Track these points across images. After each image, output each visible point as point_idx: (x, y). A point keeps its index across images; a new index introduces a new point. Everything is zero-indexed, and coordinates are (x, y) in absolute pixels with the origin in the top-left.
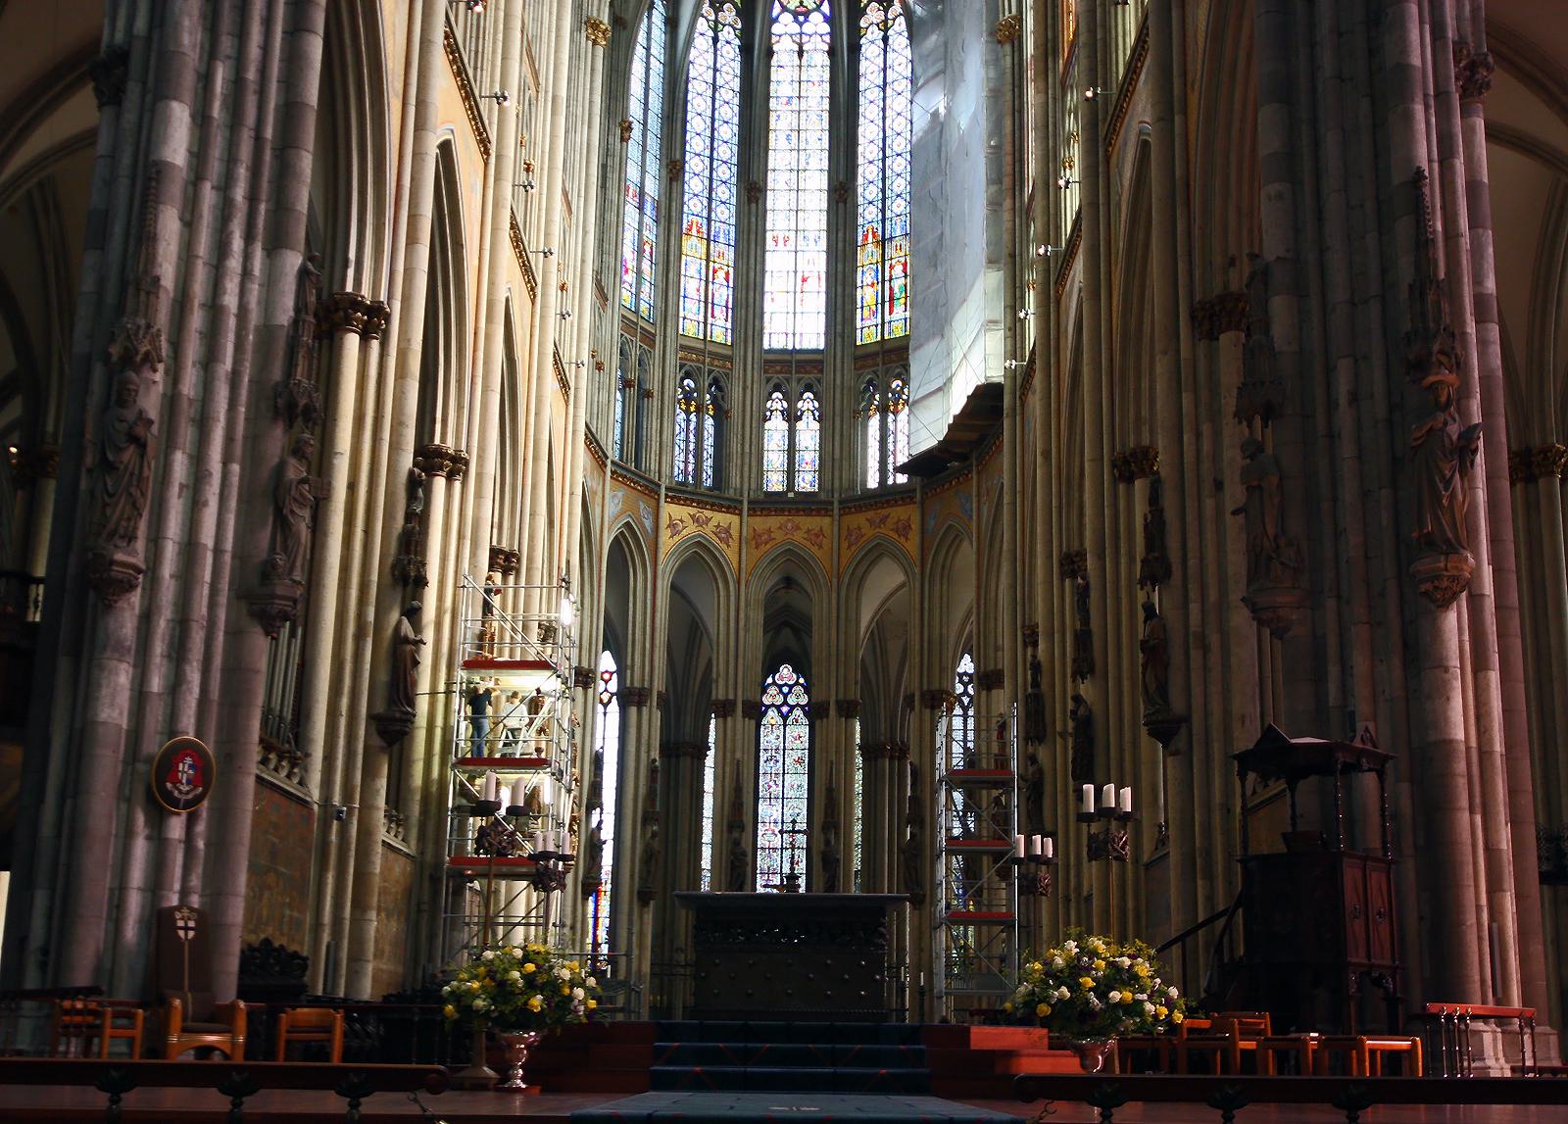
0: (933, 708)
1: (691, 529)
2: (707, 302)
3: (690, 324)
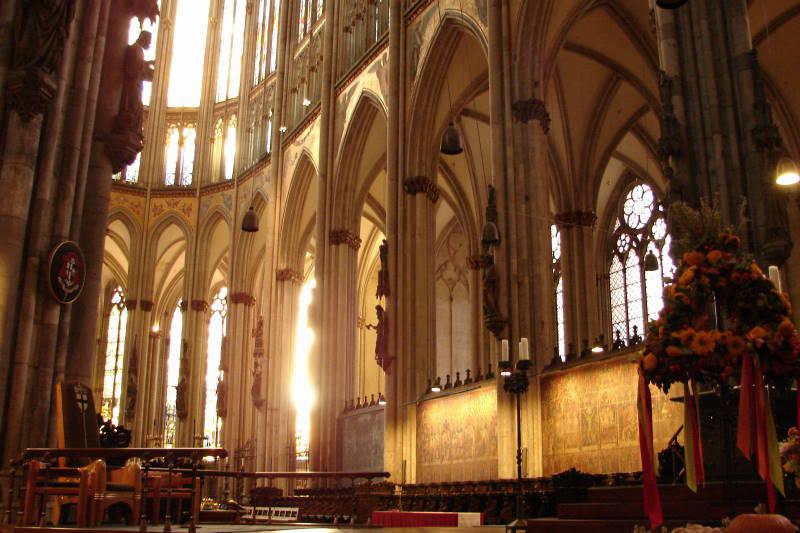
0: (198, 310)
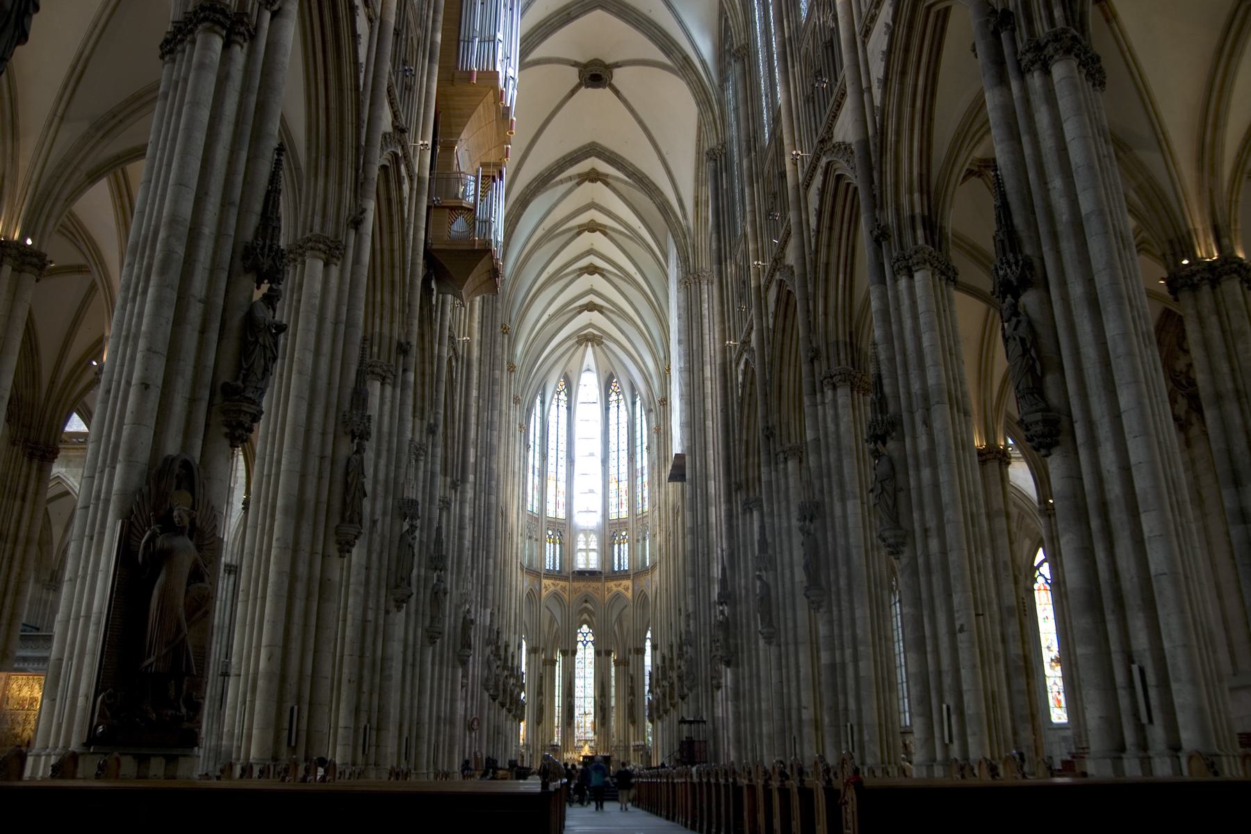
1: (552, 588)
2: (557, 504)
3: (551, 513)
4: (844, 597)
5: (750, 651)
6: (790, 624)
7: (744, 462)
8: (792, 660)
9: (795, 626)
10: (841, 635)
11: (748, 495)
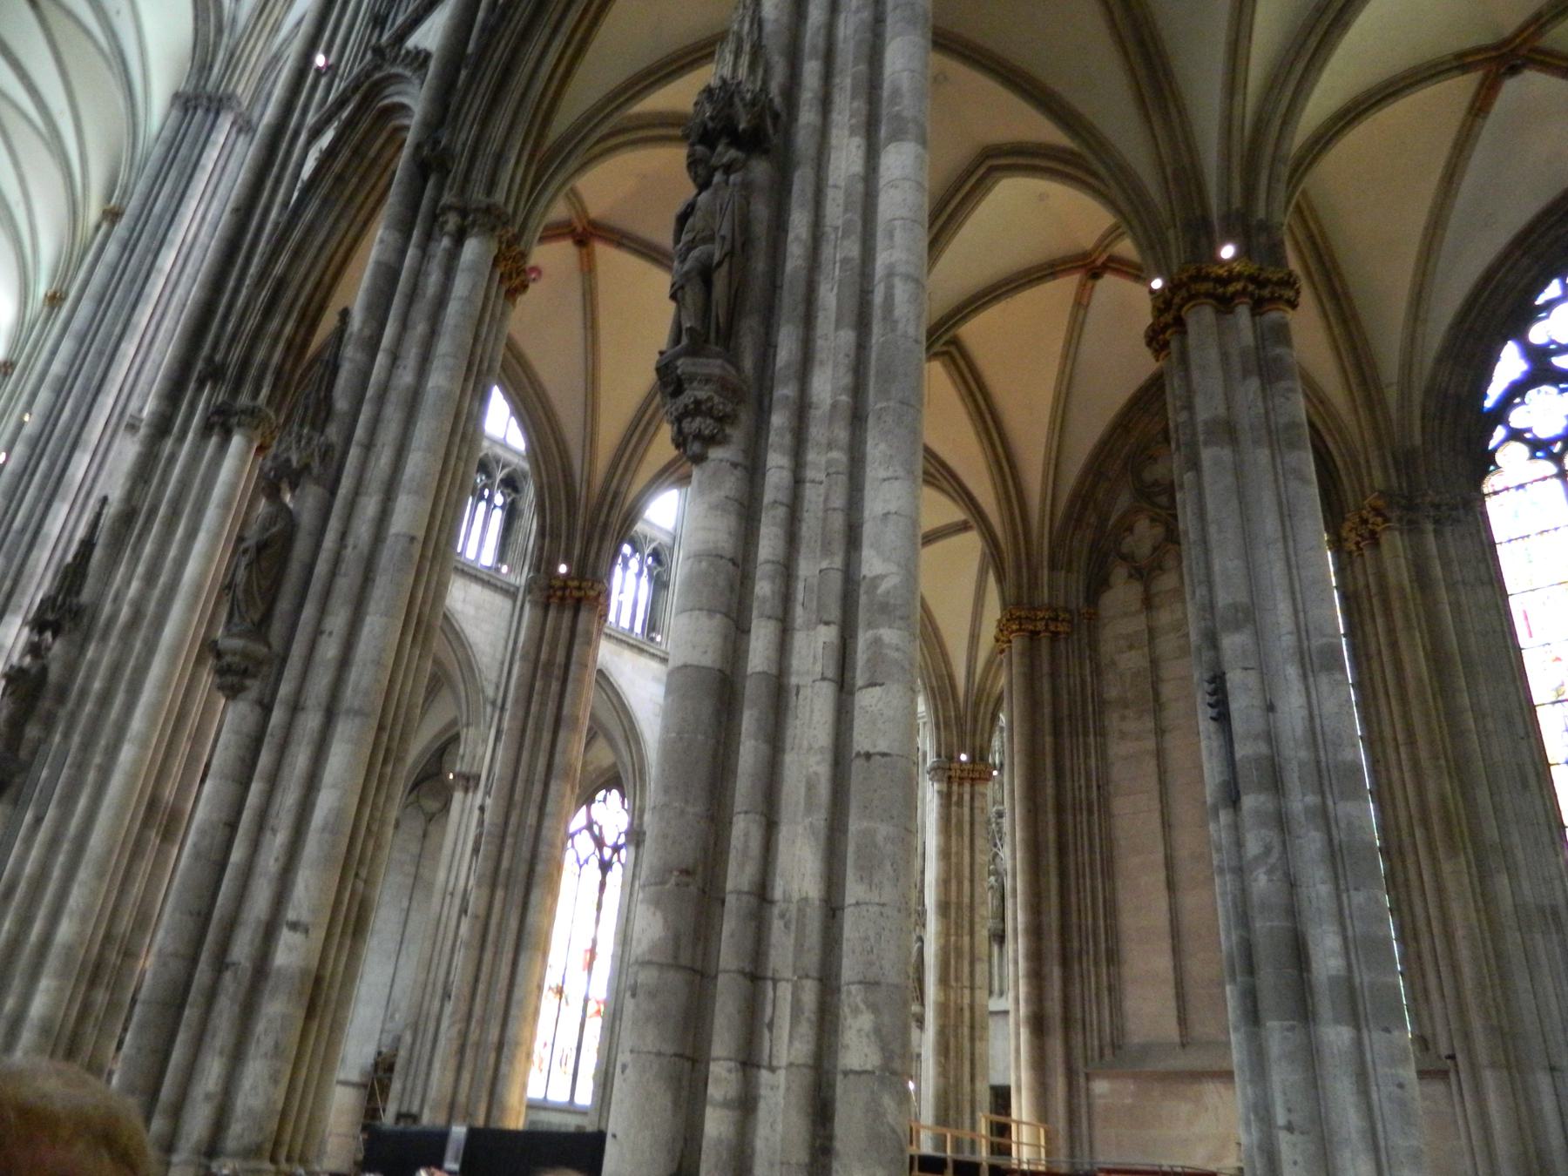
4: (826, 434)
5: (81, 767)
6: (329, 650)
7: (251, 323)
8: (300, 759)
9: (344, 662)
10: (787, 571)
11: (236, 390)
